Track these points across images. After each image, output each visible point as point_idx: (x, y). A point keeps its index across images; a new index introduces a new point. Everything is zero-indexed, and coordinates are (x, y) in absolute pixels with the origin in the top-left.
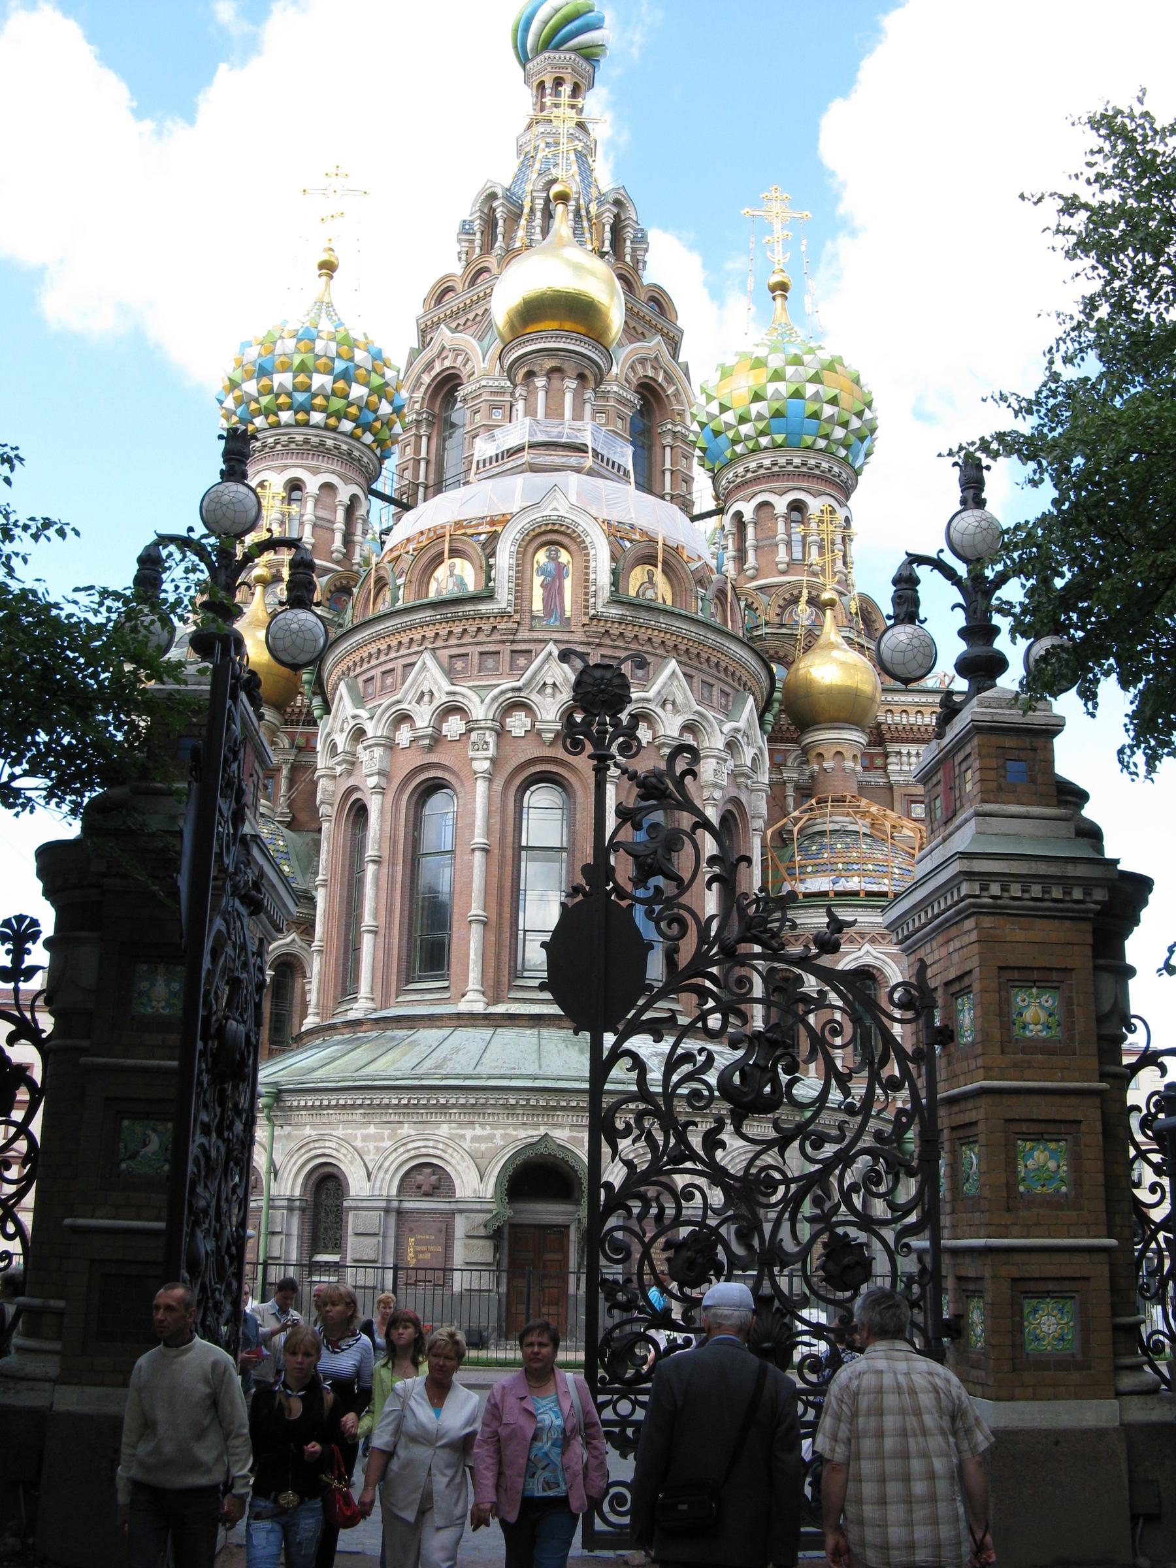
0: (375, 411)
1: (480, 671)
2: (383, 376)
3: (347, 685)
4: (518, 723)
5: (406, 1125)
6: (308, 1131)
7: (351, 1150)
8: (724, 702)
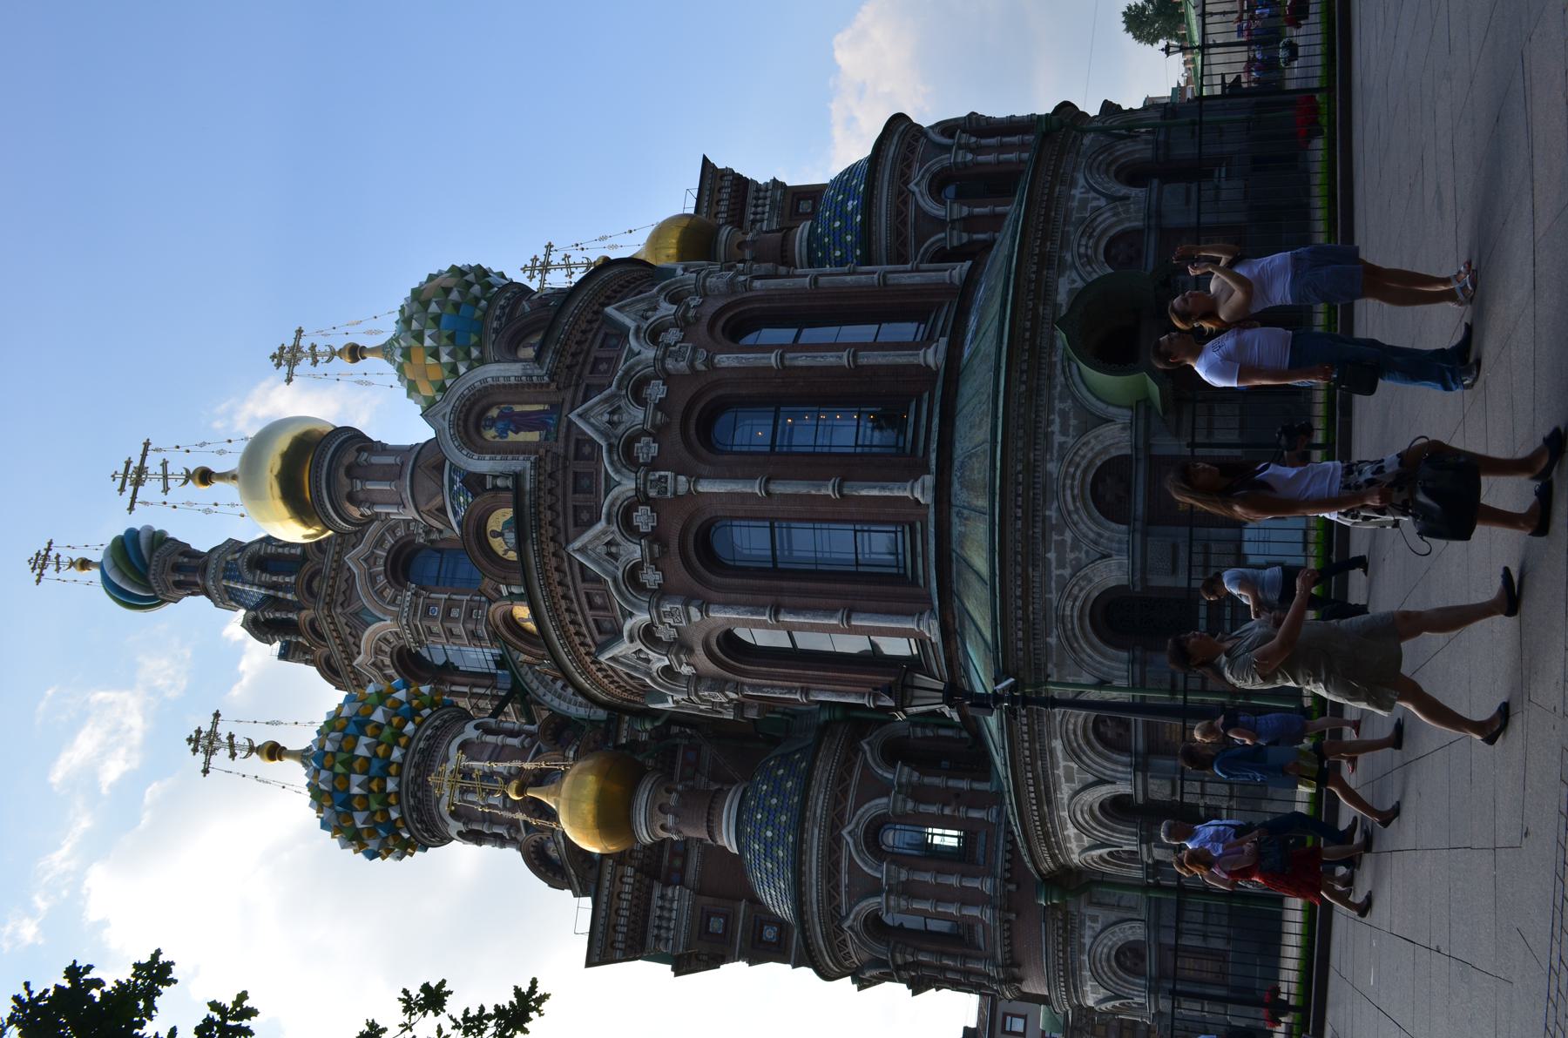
0: (402, 703)
2: (370, 694)
4: (645, 450)
5: (1047, 513)
7: (1074, 580)
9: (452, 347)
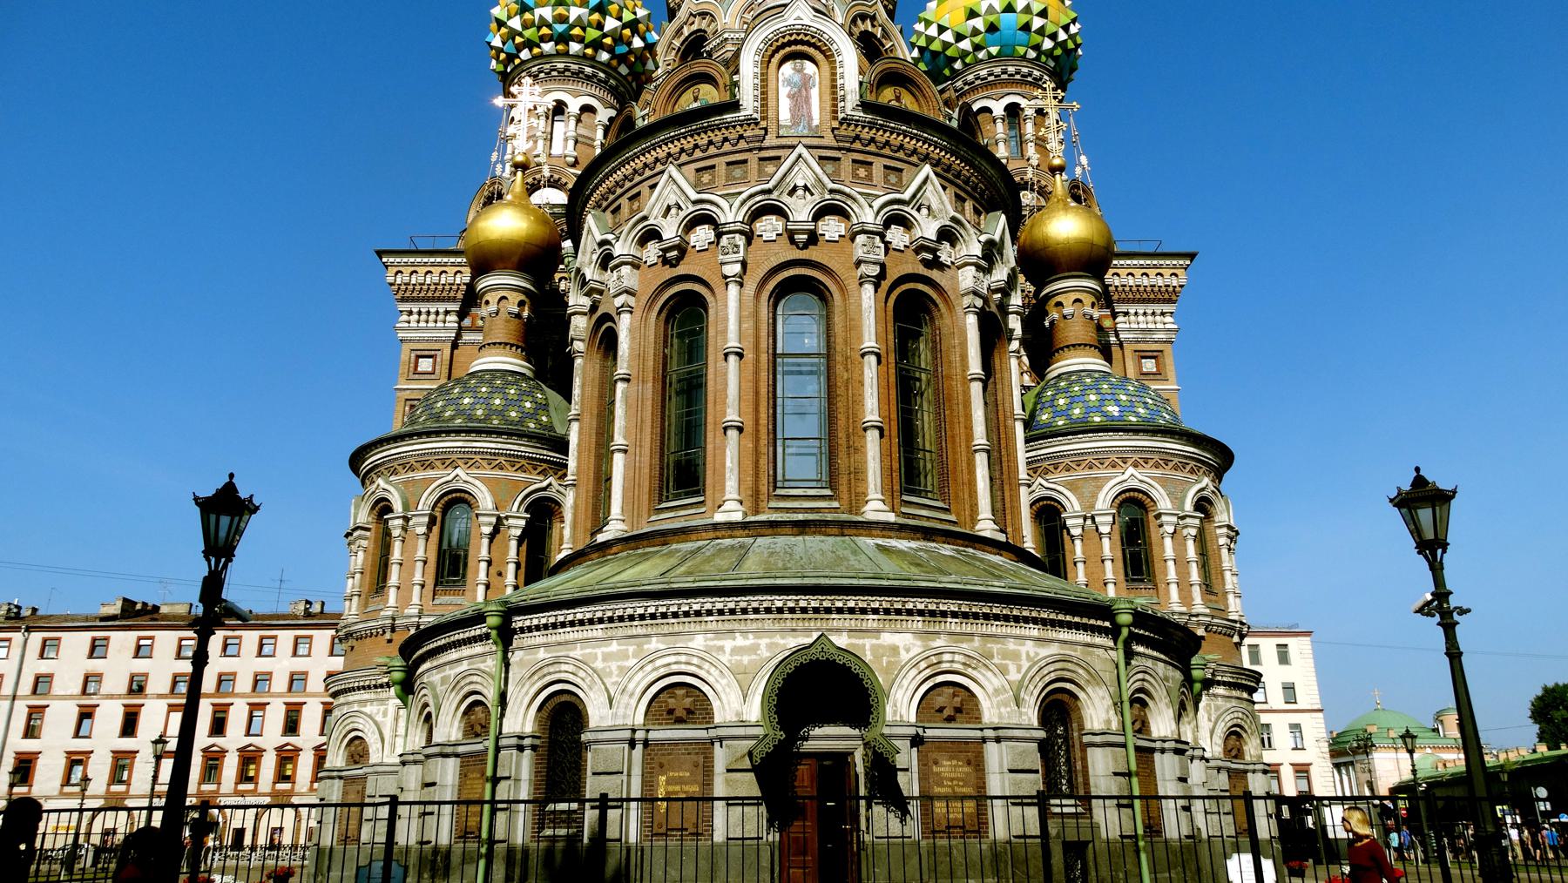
0: (629, 44)
1: (726, 181)
2: (635, 13)
3: (594, 216)
5: (654, 639)
6: (542, 654)
7: (590, 672)
8: (977, 220)
9: (983, 30)
